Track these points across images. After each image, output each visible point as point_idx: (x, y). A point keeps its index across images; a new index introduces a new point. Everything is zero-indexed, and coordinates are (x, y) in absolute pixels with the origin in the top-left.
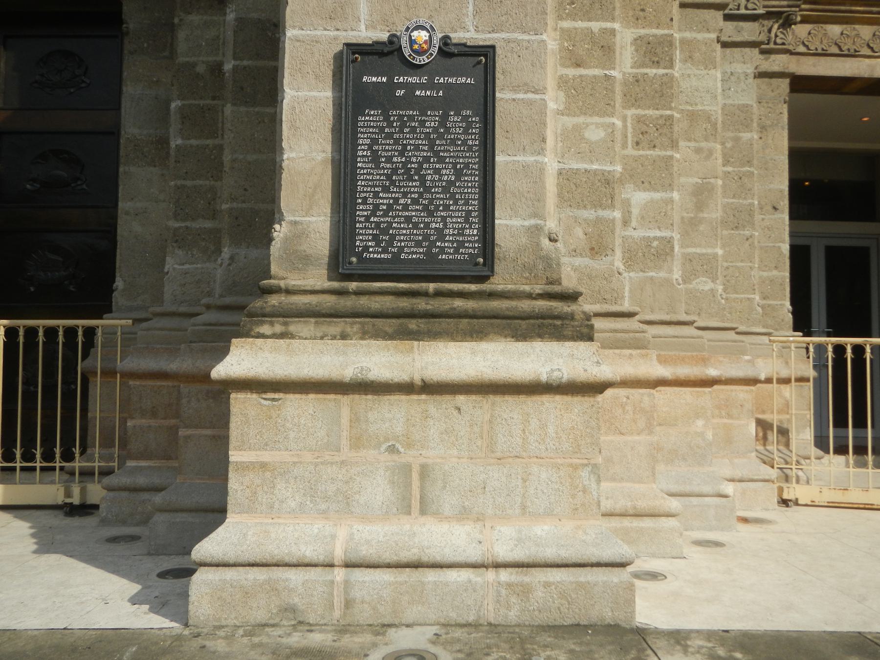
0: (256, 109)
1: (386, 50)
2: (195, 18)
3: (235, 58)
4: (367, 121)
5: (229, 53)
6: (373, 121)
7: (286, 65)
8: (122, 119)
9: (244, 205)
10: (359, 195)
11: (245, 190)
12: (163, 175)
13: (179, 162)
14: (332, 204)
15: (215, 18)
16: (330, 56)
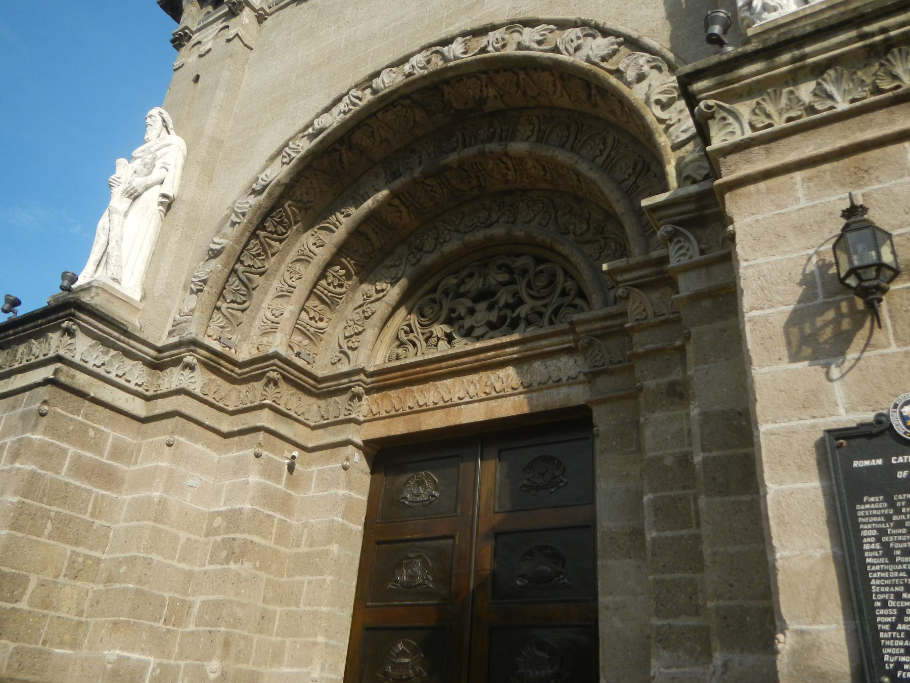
0: (732, 498)
1: (875, 430)
2: (659, 415)
3: (703, 450)
4: (868, 509)
5: (697, 445)
6: (876, 509)
7: (764, 459)
8: (598, 514)
9: (731, 603)
10: (876, 597)
11: (731, 585)
12: (638, 567)
13: (656, 555)
14: (844, 609)
15: (677, 412)
16: (811, 445)
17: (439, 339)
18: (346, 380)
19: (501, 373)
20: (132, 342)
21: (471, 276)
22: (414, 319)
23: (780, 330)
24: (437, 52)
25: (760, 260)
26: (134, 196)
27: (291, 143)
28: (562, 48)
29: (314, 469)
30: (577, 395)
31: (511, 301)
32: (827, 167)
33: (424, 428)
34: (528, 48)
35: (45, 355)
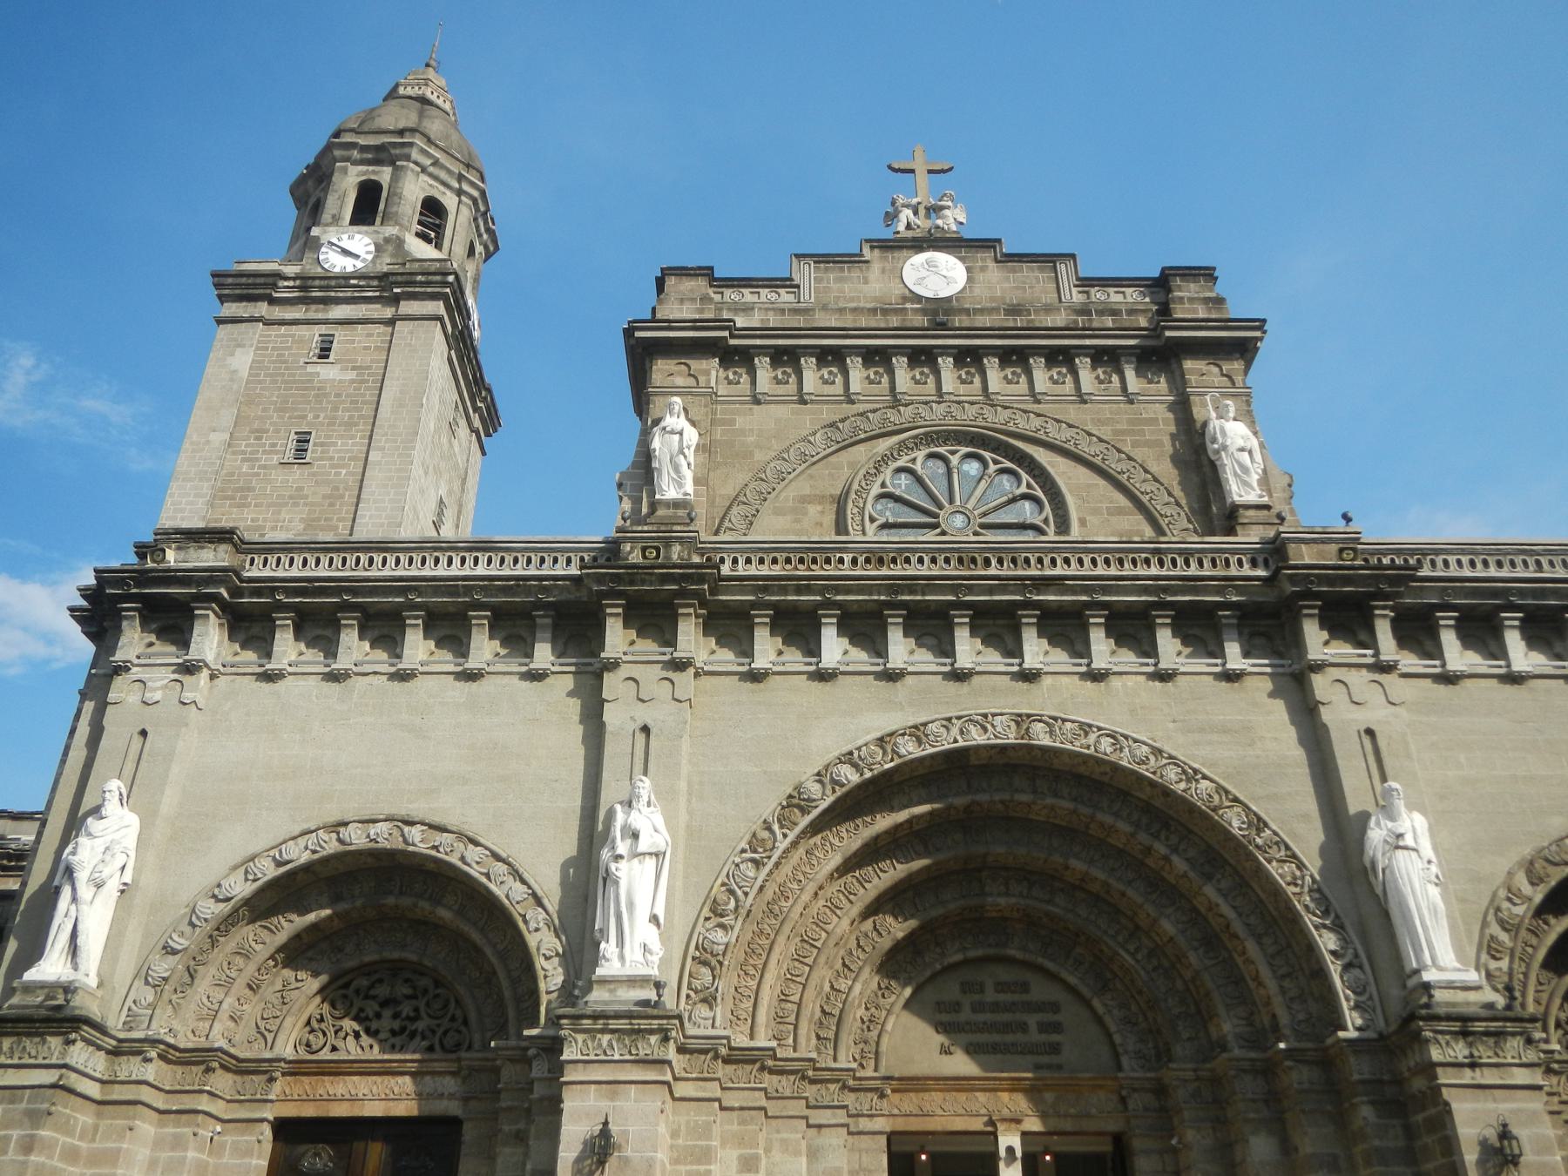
2: (507, 1150)
17: (347, 1034)
18: (266, 1064)
19: (400, 1079)
20: (106, 1039)
21: (380, 981)
22: (326, 1006)
23: (570, 1165)
24: (398, 826)
25: (570, 1128)
26: (99, 886)
27: (256, 860)
28: (492, 877)
29: (229, 1139)
30: (453, 1108)
32: (604, 1086)
33: (332, 1114)
34: (469, 865)
35: (44, 1058)
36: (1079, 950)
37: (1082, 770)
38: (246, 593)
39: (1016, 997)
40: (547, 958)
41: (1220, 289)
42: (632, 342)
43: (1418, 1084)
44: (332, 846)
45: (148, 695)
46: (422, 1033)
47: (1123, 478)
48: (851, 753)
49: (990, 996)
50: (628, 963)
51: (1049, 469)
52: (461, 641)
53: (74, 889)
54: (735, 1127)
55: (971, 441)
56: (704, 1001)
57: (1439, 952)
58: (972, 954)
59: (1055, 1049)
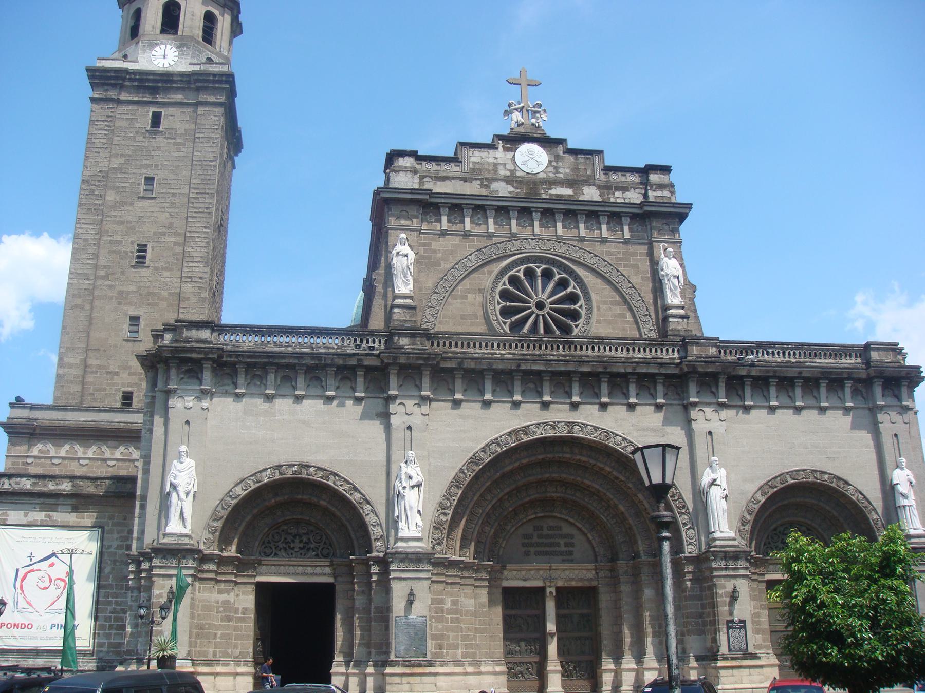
17: (281, 549)
30: (330, 580)
31: (307, 541)
36: (584, 513)
37: (593, 445)
38: (224, 356)
39: (557, 532)
40: (374, 526)
41: (673, 177)
42: (378, 197)
43: (707, 574)
44: (277, 476)
45: (186, 404)
46: (313, 549)
47: (618, 286)
48: (497, 439)
49: (545, 532)
50: (411, 532)
51: (585, 280)
52: (322, 381)
53: (178, 495)
54: (449, 589)
55: (548, 262)
56: (439, 544)
57: (721, 525)
58: (539, 515)
59: (571, 553)
